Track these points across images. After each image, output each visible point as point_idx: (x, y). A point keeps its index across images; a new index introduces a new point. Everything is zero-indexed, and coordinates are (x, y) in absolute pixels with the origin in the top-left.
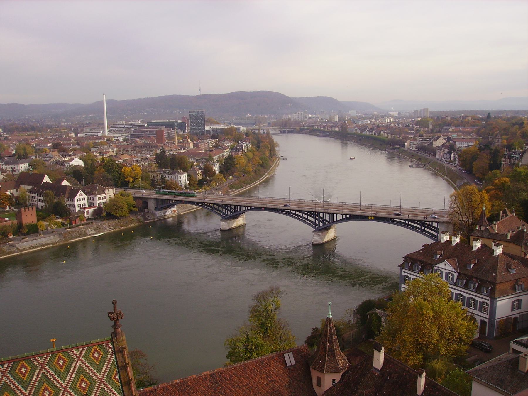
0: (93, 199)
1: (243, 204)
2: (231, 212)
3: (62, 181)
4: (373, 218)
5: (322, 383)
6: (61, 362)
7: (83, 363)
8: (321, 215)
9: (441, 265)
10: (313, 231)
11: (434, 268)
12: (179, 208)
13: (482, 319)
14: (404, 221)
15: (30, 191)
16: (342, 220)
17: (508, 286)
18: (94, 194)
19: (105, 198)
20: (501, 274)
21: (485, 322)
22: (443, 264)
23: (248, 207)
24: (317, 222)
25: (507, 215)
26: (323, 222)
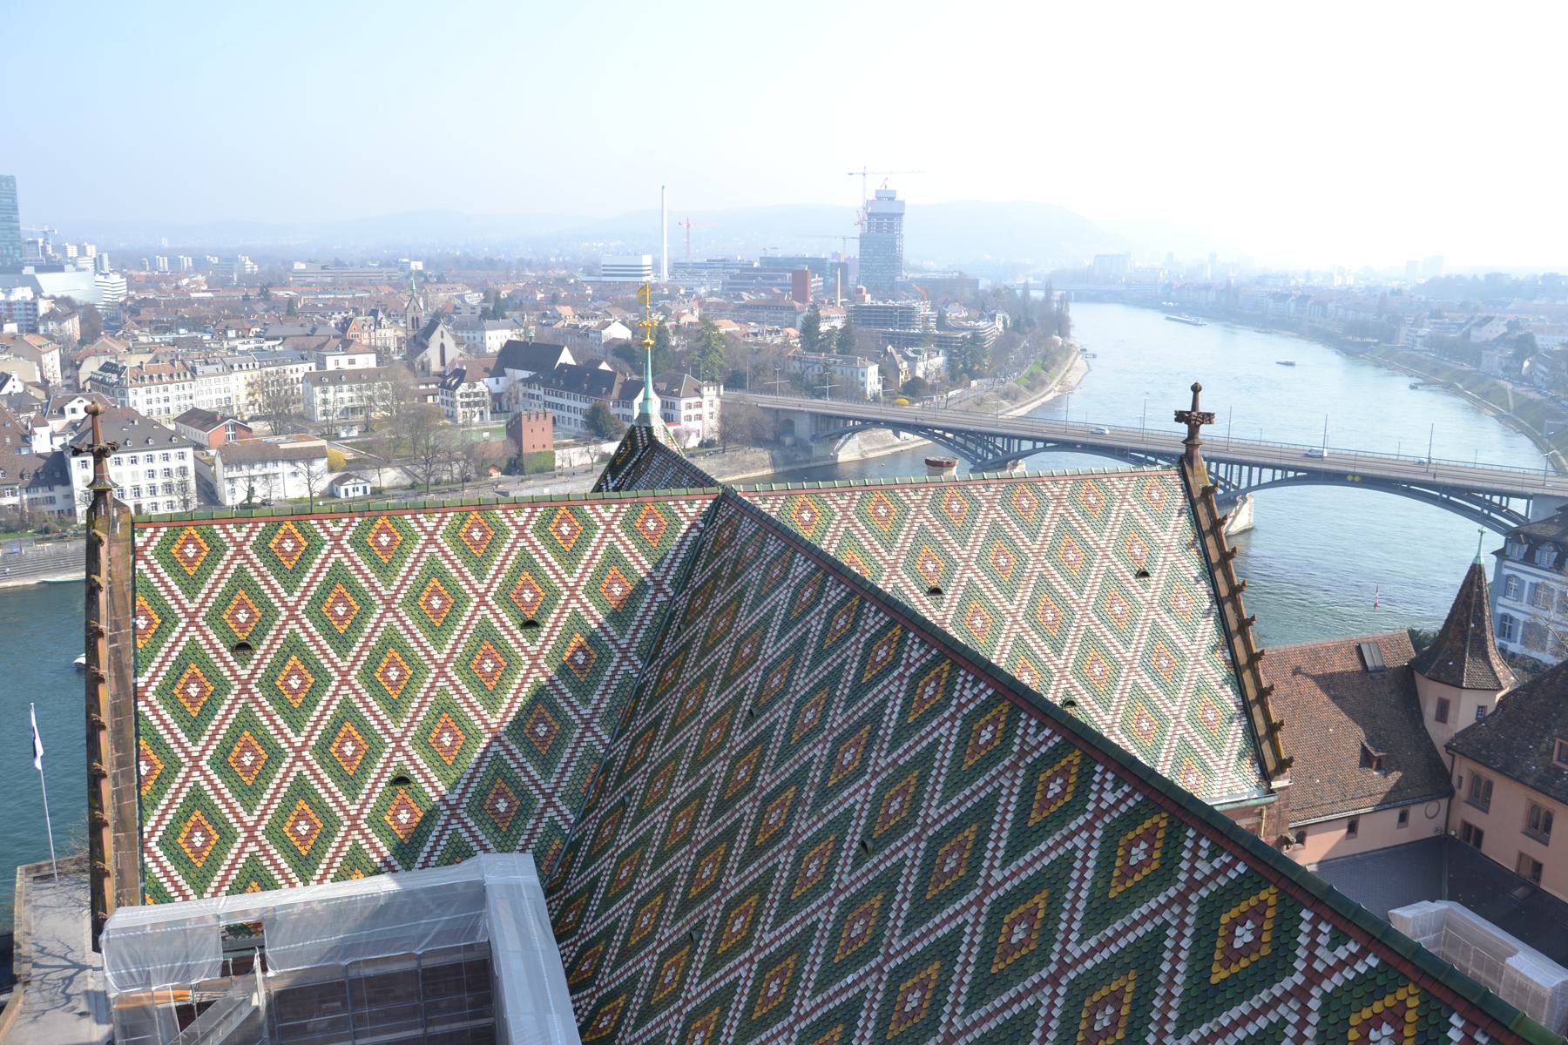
0: (673, 406)
1: (1028, 434)
3: (600, 363)
5: (1451, 713)
6: (1092, 500)
7: (1132, 505)
15: (527, 382)
16: (1274, 484)
18: (677, 395)
19: (700, 405)
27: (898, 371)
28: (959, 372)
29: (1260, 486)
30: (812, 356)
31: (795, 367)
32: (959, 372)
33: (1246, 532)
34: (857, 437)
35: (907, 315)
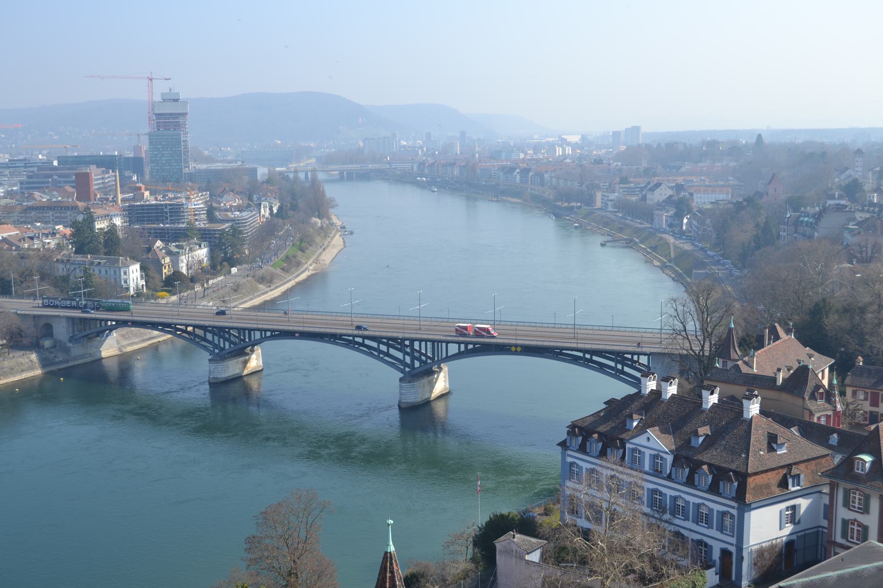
1: (255, 326)
2: (231, 342)
4: (519, 349)
8: (416, 345)
9: (641, 440)
10: (401, 380)
11: (628, 446)
12: (123, 336)
13: (724, 546)
14: (581, 354)
16: (459, 355)
17: (774, 478)
20: (758, 455)
21: (730, 553)
22: (645, 436)
23: (266, 330)
24: (408, 359)
25: (777, 337)
26: (419, 359)
27: (160, 266)
28: (222, 259)
29: (448, 358)
30: (79, 258)
31: (61, 270)
32: (222, 259)
33: (442, 396)
34: (114, 334)
35: (176, 211)
